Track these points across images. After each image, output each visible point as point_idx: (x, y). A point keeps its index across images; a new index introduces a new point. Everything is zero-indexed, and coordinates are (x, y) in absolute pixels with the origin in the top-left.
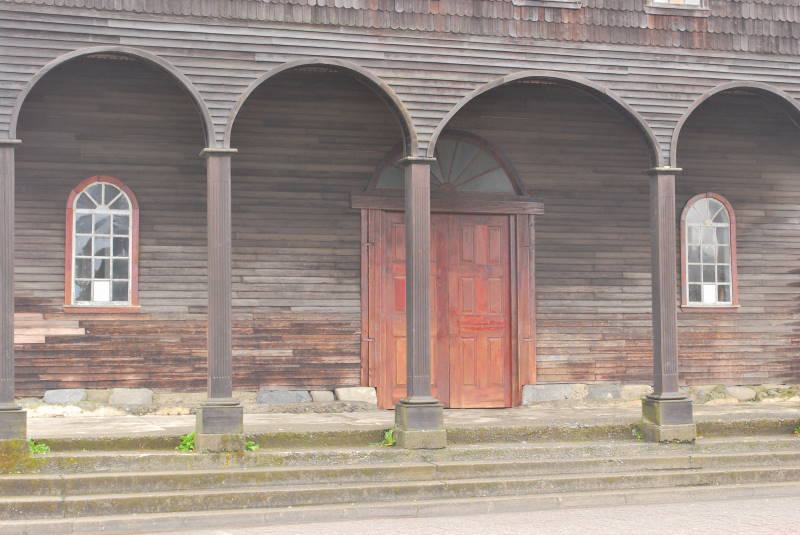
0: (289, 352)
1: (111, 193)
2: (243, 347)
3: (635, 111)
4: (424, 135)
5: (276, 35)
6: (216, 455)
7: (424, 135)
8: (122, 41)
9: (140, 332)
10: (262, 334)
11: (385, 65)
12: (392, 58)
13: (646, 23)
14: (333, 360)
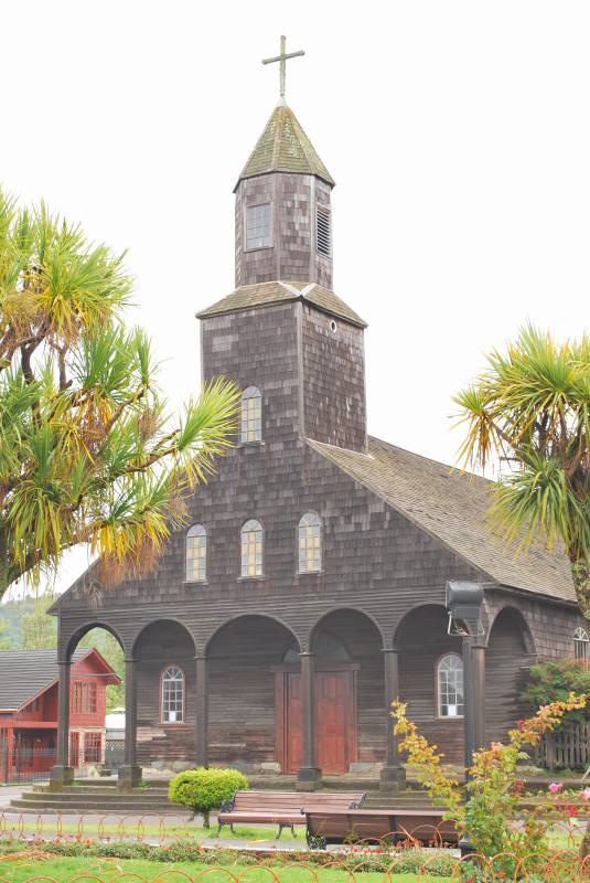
0: (244, 745)
2: (225, 741)
4: (200, 647)
5: (147, 609)
6: (121, 788)
7: (200, 647)
9: (187, 735)
10: (234, 737)
13: (296, 583)
14: (261, 749)
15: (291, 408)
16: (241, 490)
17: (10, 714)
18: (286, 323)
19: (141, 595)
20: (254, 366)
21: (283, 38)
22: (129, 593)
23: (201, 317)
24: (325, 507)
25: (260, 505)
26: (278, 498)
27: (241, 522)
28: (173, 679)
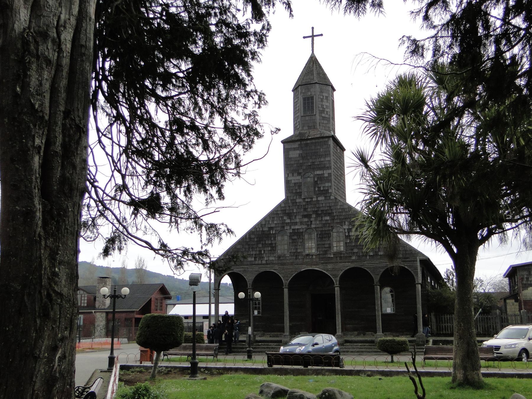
4: (286, 282)
7: (286, 282)
13: (332, 256)
15: (328, 182)
16: (305, 216)
17: (133, 312)
18: (325, 147)
19: (255, 260)
20: (309, 164)
21: (313, 28)
22: (249, 259)
23: (284, 142)
24: (345, 224)
25: (313, 223)
26: (322, 220)
27: (304, 230)
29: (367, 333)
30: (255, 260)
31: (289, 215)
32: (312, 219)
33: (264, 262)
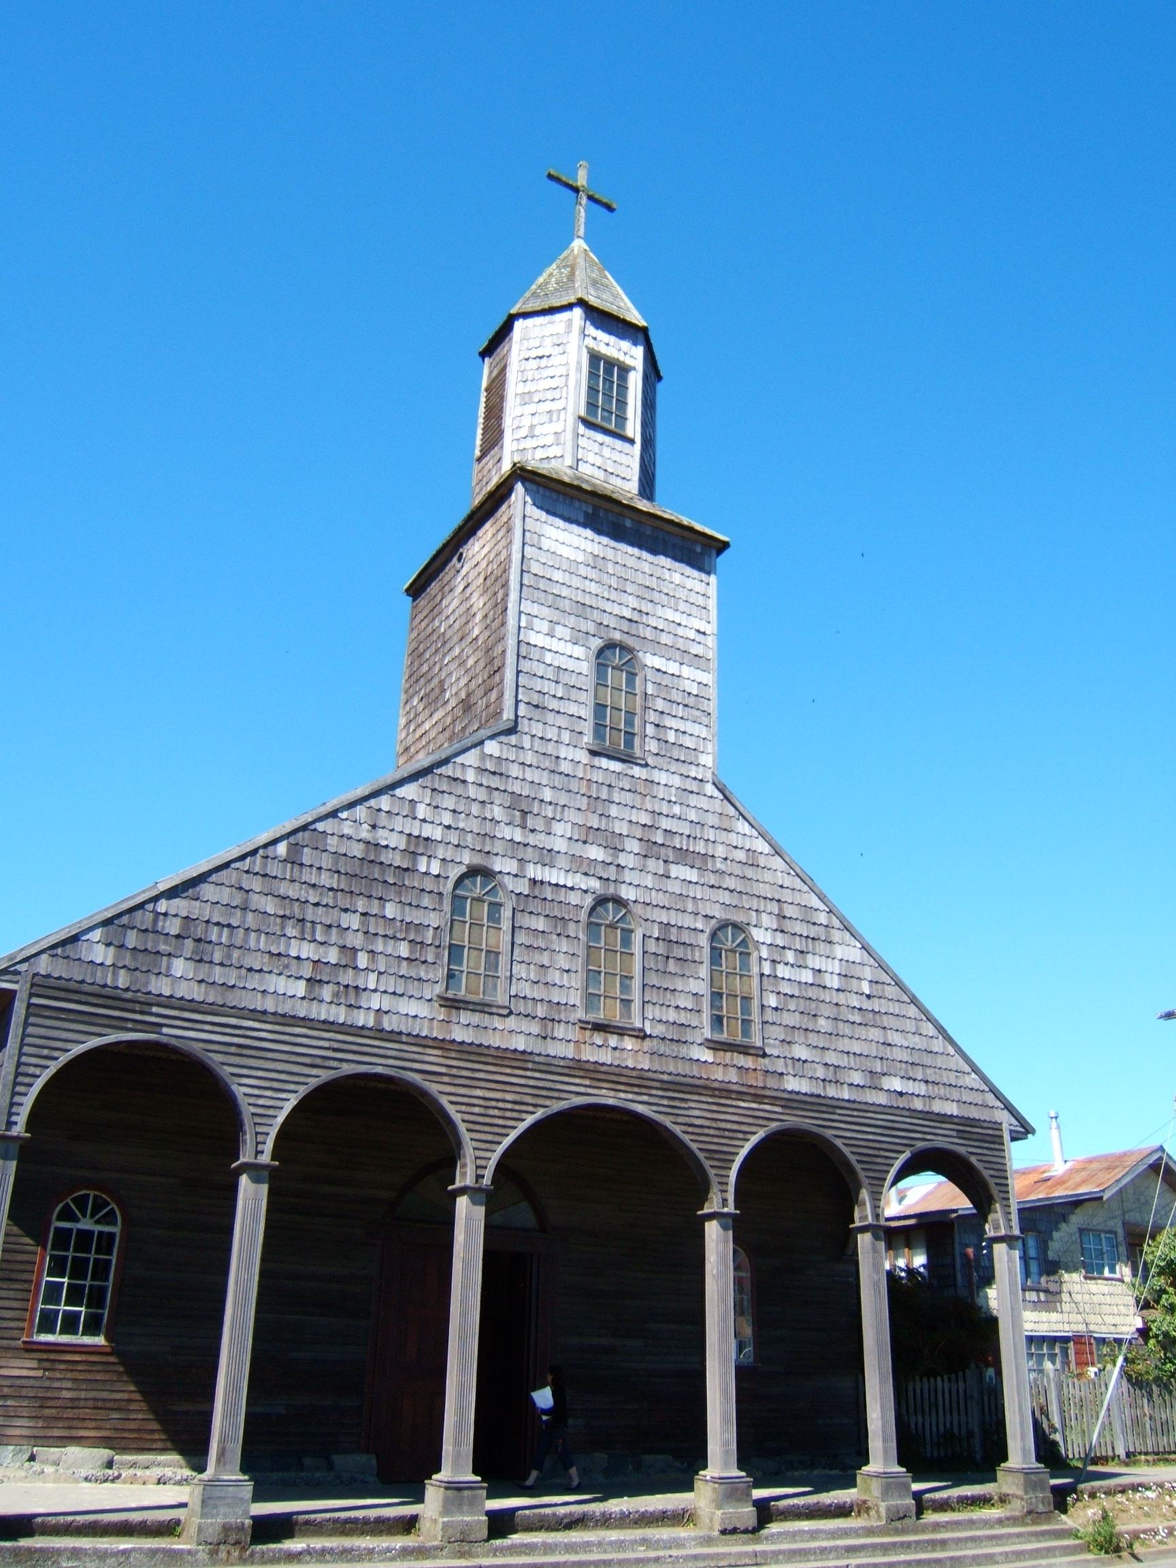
1: (98, 1207)
3: (694, 1146)
8: (165, 1030)
11: (446, 1079)
12: (454, 1071)
16: (588, 835)
28: (86, 1224)
29: (648, 1458)
30: (310, 998)
31: (521, 809)
32: (623, 859)
33: (362, 1019)
